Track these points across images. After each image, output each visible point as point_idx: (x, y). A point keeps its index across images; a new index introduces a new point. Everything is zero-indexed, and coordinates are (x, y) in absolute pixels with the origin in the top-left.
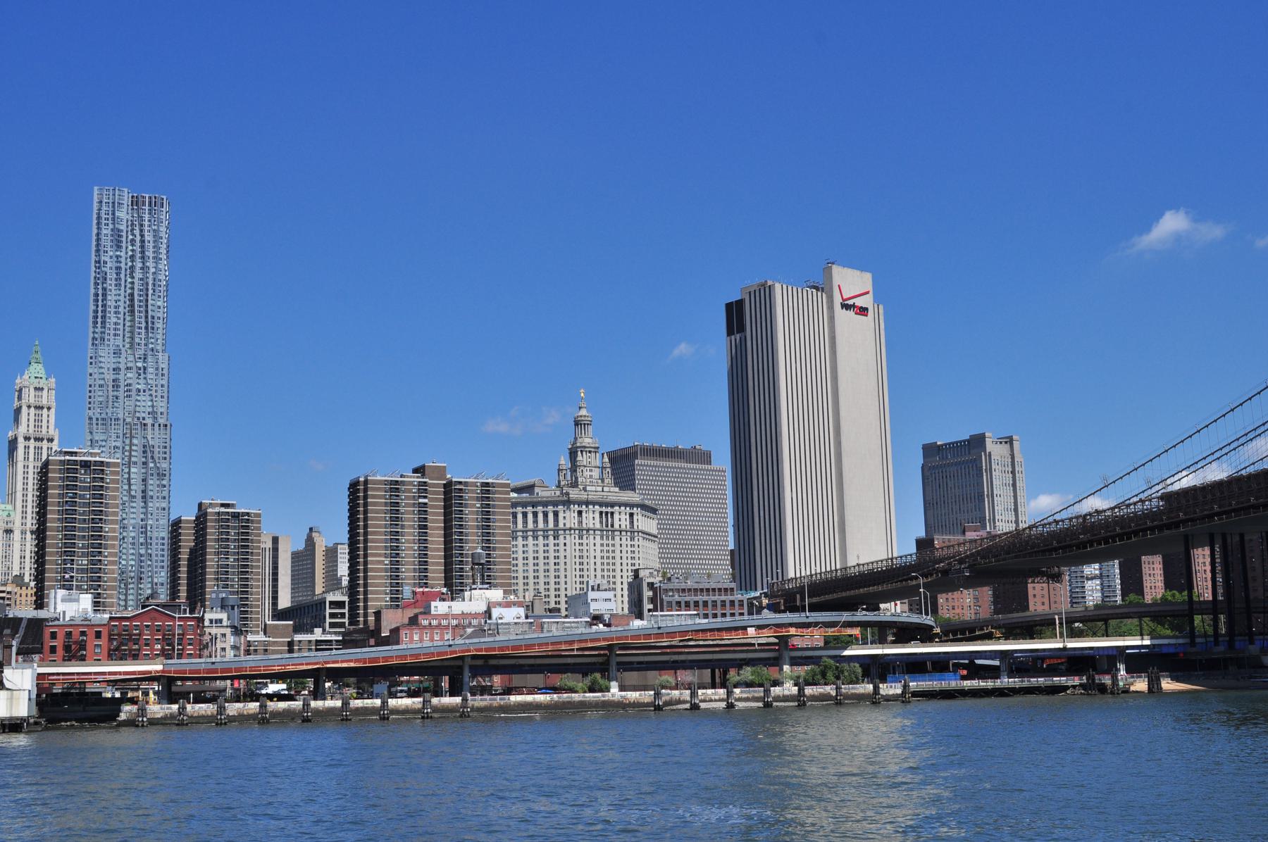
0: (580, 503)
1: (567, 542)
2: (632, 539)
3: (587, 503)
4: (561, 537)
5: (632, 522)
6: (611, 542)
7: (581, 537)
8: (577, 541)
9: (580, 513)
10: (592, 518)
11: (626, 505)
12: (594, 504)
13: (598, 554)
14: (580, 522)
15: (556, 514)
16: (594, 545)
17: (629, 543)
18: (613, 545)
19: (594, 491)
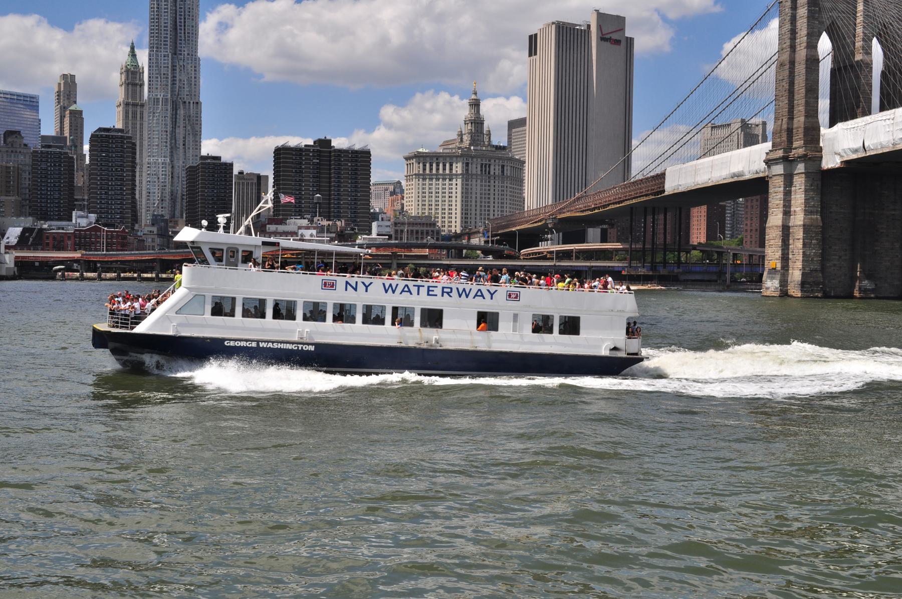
5: (503, 172)
13: (479, 192)
14: (467, 170)
15: (451, 165)
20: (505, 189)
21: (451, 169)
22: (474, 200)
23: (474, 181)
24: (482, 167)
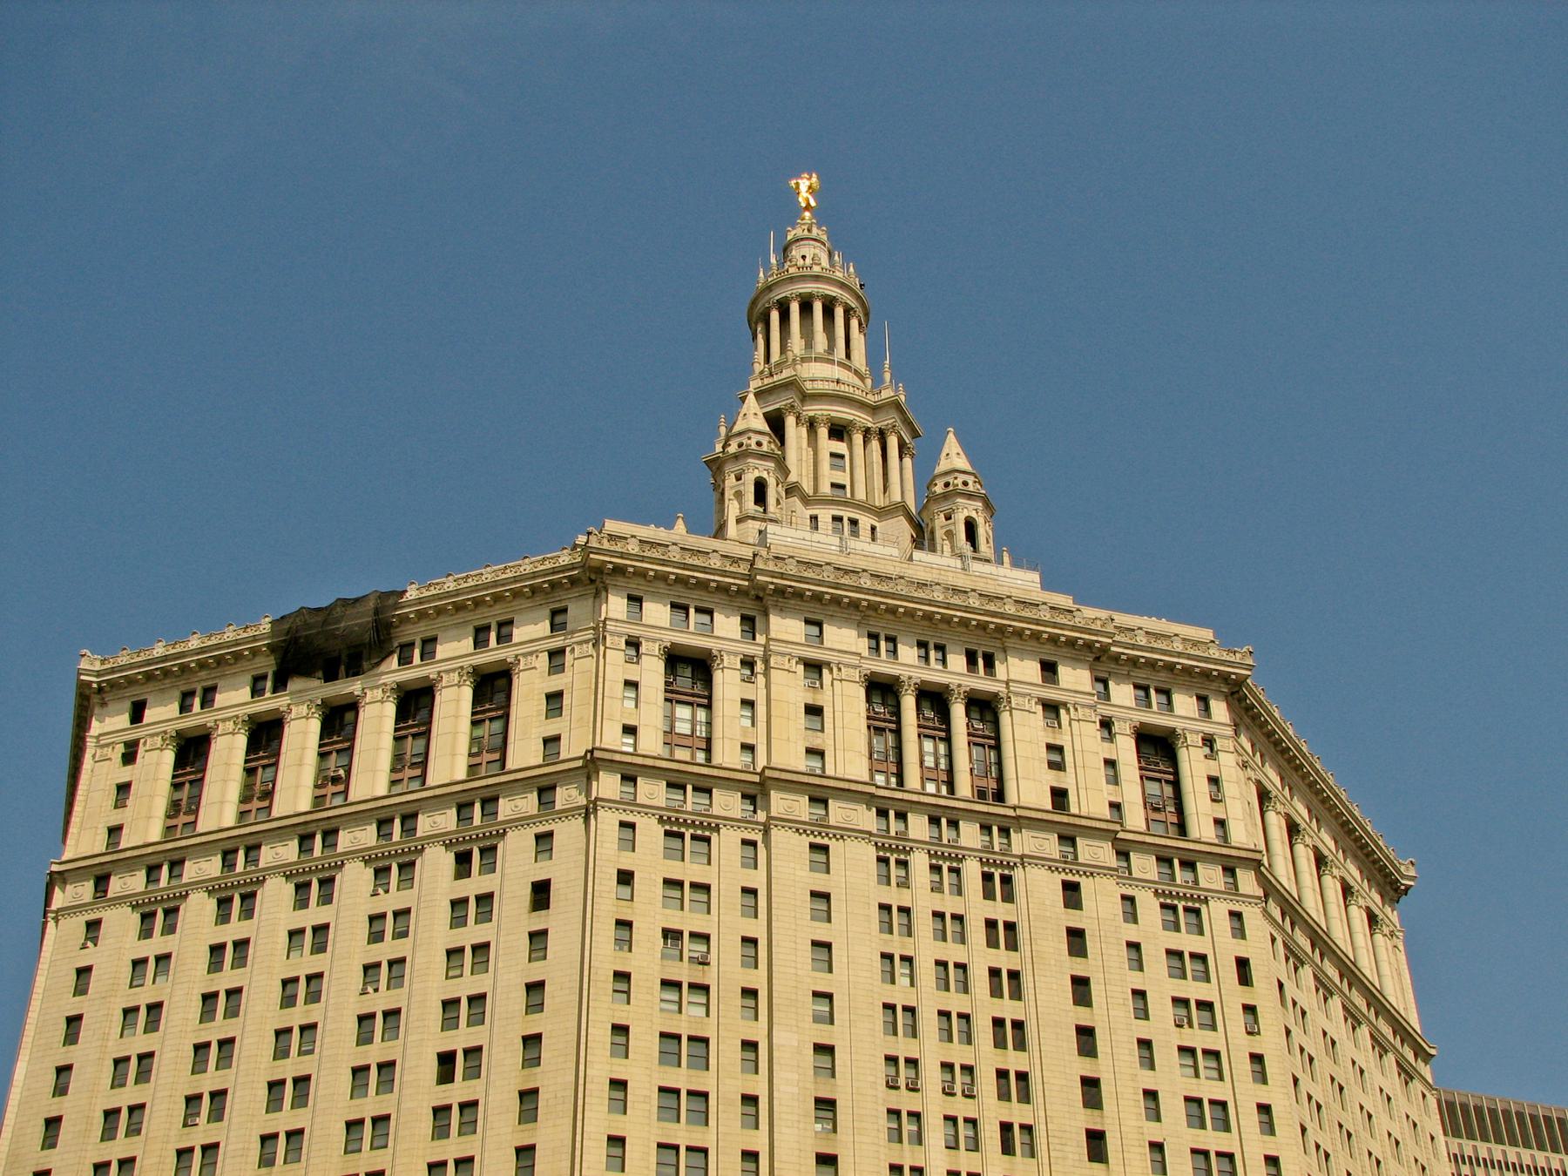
0: (692, 593)
1: (561, 870)
2: (1184, 910)
3: (757, 601)
4: (517, 849)
6: (977, 908)
8: (651, 857)
9: (691, 670)
10: (794, 708)
11: (1104, 662)
12: (818, 607)
15: (492, 687)
16: (826, 926)
18: (1004, 934)
21: (491, 745)
22: (793, 1084)
23: (790, 848)
24: (885, 724)
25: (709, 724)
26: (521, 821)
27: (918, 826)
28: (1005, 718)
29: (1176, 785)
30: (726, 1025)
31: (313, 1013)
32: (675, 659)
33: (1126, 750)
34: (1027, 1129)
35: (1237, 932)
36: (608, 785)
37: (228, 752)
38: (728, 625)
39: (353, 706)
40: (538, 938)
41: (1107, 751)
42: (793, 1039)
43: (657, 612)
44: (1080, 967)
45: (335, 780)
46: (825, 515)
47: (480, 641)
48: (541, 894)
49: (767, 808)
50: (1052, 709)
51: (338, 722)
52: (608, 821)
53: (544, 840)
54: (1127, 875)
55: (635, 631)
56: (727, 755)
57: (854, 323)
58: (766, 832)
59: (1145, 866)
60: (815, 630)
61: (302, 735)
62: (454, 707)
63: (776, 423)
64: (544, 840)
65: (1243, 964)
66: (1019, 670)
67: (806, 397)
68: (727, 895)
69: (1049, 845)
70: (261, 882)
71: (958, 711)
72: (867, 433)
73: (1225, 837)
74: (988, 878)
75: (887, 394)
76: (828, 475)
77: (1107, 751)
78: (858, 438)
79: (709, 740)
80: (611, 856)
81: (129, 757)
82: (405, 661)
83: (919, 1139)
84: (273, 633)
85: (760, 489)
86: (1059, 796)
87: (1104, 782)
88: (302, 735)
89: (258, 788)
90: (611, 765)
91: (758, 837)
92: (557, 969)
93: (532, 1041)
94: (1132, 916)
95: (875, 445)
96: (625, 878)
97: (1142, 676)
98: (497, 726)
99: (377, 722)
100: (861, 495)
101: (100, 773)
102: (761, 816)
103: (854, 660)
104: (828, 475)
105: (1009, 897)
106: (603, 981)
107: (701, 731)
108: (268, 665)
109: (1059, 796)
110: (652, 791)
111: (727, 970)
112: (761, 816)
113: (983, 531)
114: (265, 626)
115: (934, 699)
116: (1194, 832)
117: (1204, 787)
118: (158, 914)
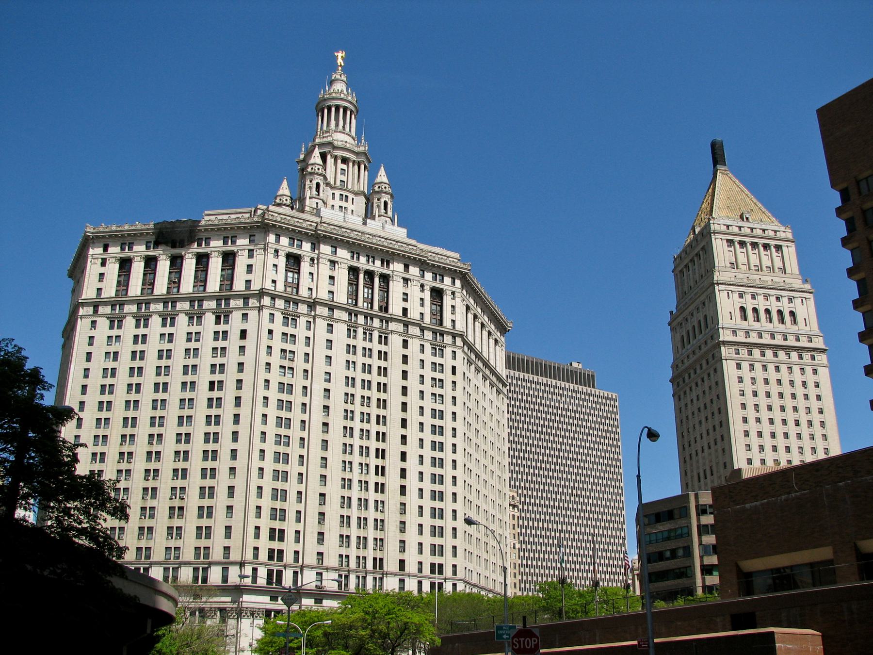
0: (296, 235)
1: (251, 327)
2: (437, 350)
3: (317, 239)
4: (236, 316)
6: (376, 347)
7: (290, 318)
8: (278, 327)
9: (294, 261)
10: (326, 277)
11: (424, 265)
12: (336, 242)
15: (229, 259)
17: (428, 357)
19: (340, 212)
20: (447, 377)
21: (228, 279)
23: (321, 324)
24: (353, 282)
25: (298, 279)
26: (239, 309)
27: (361, 319)
28: (391, 283)
29: (441, 307)
30: (299, 382)
31: (169, 363)
32: (289, 256)
33: (427, 295)
34: (384, 417)
35: (454, 358)
36: (266, 301)
37: (138, 268)
38: (307, 246)
39: (181, 258)
40: (242, 348)
41: (421, 295)
42: (318, 386)
43: (285, 241)
44: (405, 367)
45: (175, 282)
46: (338, 193)
47: (225, 243)
48: (243, 334)
49: (315, 311)
50: (406, 280)
51: (176, 263)
52: (266, 313)
53: (245, 316)
54: (422, 337)
55: (277, 247)
56: (304, 292)
57: (353, 116)
58: (314, 319)
59: (428, 335)
60: (334, 249)
61: (164, 266)
62: (216, 264)
63: (324, 157)
64: (245, 316)
65: (454, 368)
66: (397, 267)
67: (335, 148)
68: (300, 340)
69: (400, 327)
70: (151, 316)
71: (377, 280)
72: (354, 162)
73: (454, 326)
74: (380, 337)
75: (362, 149)
76: (340, 177)
77: (421, 295)
78: (351, 164)
79: (298, 285)
80: (266, 325)
81: (103, 264)
82: (199, 245)
83: (352, 419)
84: (155, 228)
85: (318, 185)
86: (405, 310)
87: (419, 306)
88: (164, 266)
89: (149, 282)
90: (268, 294)
91: (312, 320)
92: (248, 359)
93: (239, 382)
94: (422, 351)
95: (356, 167)
96: (270, 332)
97: (435, 270)
98: (230, 272)
99: (189, 265)
100: (350, 186)
101: (92, 269)
102: (313, 313)
103: (345, 261)
104: (340, 177)
105: (386, 344)
106: (263, 366)
107: (296, 281)
108: (152, 238)
109: (405, 310)
110: (280, 304)
111: (299, 364)
112: (313, 313)
113: (390, 205)
114: (152, 226)
115: (370, 274)
116: (445, 324)
117: (450, 308)
118: (116, 321)
